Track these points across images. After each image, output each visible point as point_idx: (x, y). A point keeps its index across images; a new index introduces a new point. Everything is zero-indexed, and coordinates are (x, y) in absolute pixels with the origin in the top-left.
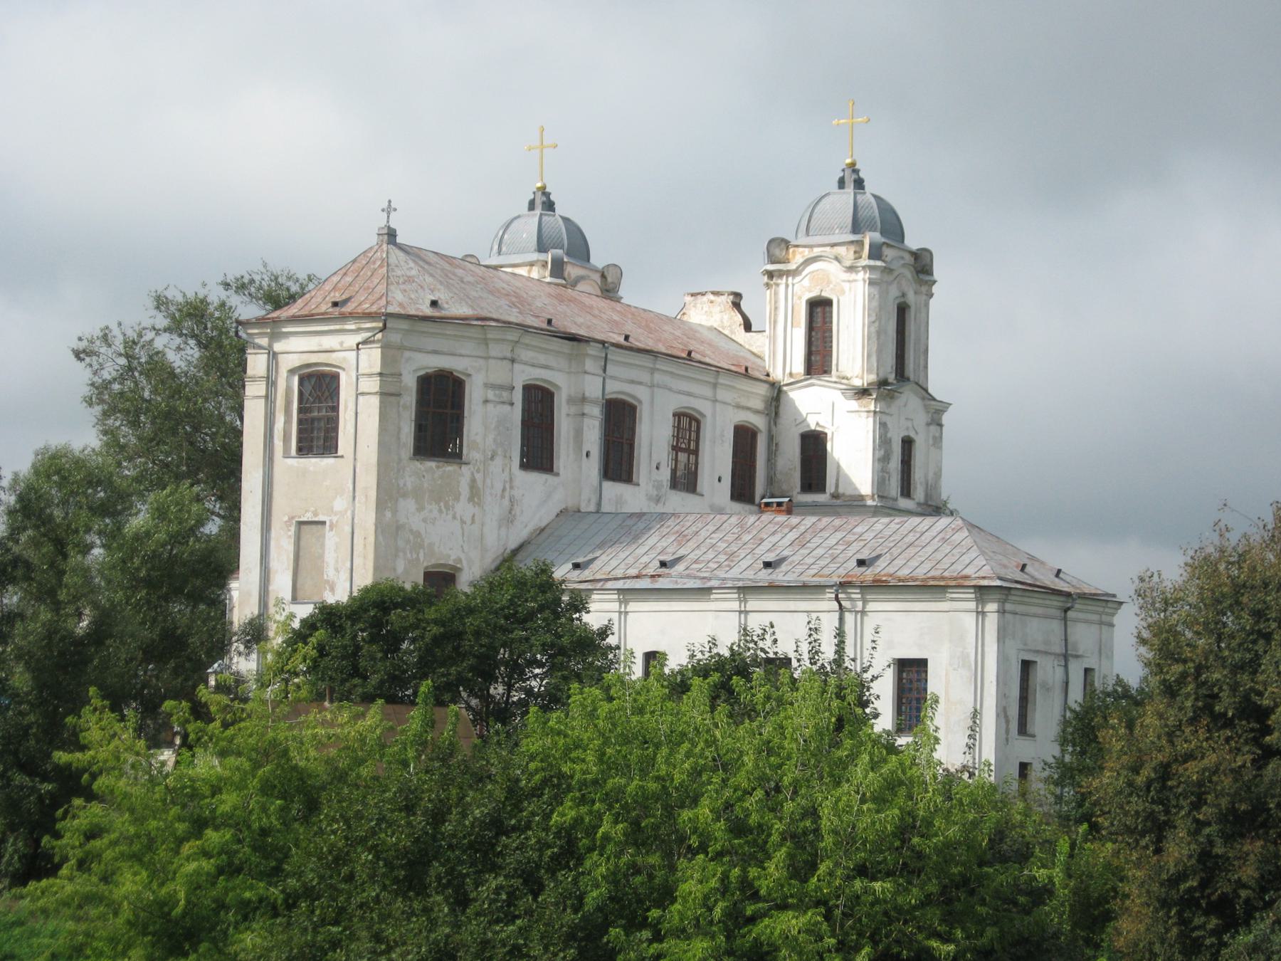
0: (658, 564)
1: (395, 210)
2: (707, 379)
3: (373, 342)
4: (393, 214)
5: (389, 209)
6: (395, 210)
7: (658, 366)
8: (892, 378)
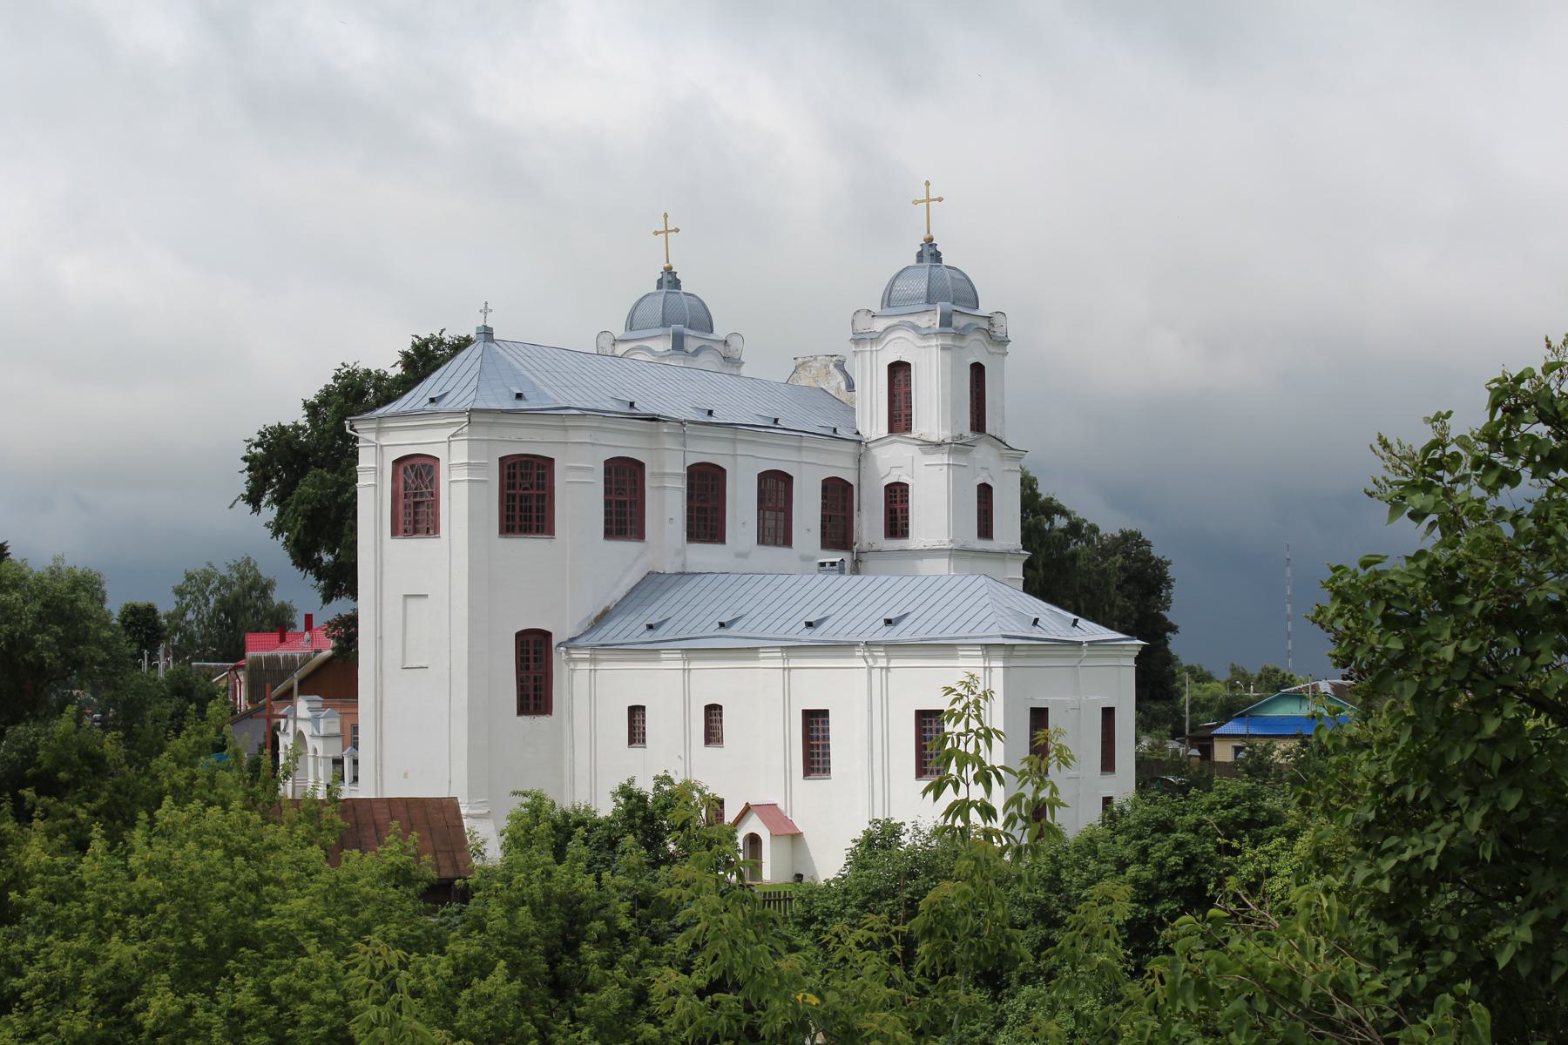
0: (718, 626)
3: (462, 434)
4: (489, 314)
5: (486, 310)
6: (491, 311)
8: (967, 431)
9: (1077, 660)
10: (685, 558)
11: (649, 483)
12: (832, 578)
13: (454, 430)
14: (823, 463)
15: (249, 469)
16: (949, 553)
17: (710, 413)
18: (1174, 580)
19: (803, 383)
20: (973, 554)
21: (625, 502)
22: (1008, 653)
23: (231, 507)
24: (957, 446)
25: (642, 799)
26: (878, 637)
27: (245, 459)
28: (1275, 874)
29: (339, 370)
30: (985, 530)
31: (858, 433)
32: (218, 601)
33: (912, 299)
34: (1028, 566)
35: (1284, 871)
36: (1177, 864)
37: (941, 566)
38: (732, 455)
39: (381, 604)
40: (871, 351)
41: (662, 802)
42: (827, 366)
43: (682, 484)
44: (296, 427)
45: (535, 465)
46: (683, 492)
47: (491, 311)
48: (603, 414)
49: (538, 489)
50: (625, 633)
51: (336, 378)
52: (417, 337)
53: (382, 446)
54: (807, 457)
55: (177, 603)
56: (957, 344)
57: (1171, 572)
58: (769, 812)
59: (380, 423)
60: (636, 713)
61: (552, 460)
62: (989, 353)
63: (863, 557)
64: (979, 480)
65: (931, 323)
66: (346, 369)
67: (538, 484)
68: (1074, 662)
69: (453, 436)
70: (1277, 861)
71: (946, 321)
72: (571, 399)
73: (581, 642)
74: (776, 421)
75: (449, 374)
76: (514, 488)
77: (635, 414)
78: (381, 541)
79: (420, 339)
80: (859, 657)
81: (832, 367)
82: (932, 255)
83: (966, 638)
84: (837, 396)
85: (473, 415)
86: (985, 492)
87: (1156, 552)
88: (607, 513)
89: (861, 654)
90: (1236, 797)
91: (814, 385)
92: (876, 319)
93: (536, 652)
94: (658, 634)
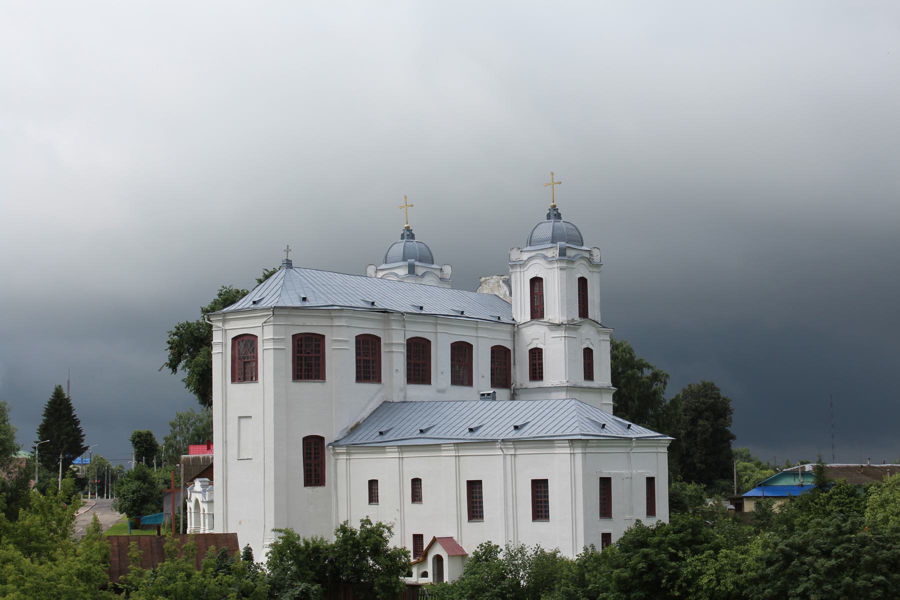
0: (419, 432)
1: (290, 250)
2: (472, 326)
3: (270, 322)
4: (289, 252)
5: (288, 250)
6: (290, 250)
7: (438, 322)
9: (630, 449)
10: (406, 394)
11: (383, 349)
12: (487, 402)
13: (265, 319)
14: (492, 337)
15: (171, 348)
16: (566, 388)
17: (421, 308)
18: (733, 409)
19: (485, 292)
20: (581, 389)
21: (369, 360)
22: (585, 445)
23: (160, 370)
24: (570, 326)
25: (354, 533)
26: (510, 436)
27: (169, 342)
28: (705, 573)
29: (221, 290)
30: (589, 374)
31: (513, 320)
32: (194, 430)
33: (542, 241)
34: (617, 397)
35: (710, 572)
36: (643, 568)
37: (563, 395)
38: (435, 333)
39: (226, 422)
40: (520, 272)
41: (364, 535)
42: (498, 282)
43: (403, 350)
44: (198, 323)
45: (314, 340)
46: (404, 355)
47: (285, 251)
48: (354, 309)
49: (316, 353)
50: (366, 438)
51: (220, 295)
52: (266, 270)
53: (226, 330)
54: (481, 333)
55: (171, 431)
56: (569, 266)
57: (732, 405)
58: (448, 542)
59: (224, 317)
60: (373, 484)
61: (323, 336)
62: (590, 271)
63: (517, 392)
64: (585, 346)
65: (554, 255)
66: (225, 290)
67: (315, 350)
68: (628, 450)
69: (265, 323)
70: (707, 565)
71: (563, 253)
72: (335, 300)
73: (341, 443)
74: (462, 313)
75: (265, 288)
76: (301, 353)
77: (374, 309)
78: (226, 385)
79: (268, 272)
80: (498, 449)
81: (501, 282)
82: (555, 215)
83: (560, 436)
84: (504, 299)
85: (275, 310)
86: (588, 354)
87: (723, 395)
88: (357, 367)
89: (499, 446)
90: (683, 526)
91: (491, 293)
92: (523, 253)
93: (315, 449)
94: (386, 437)
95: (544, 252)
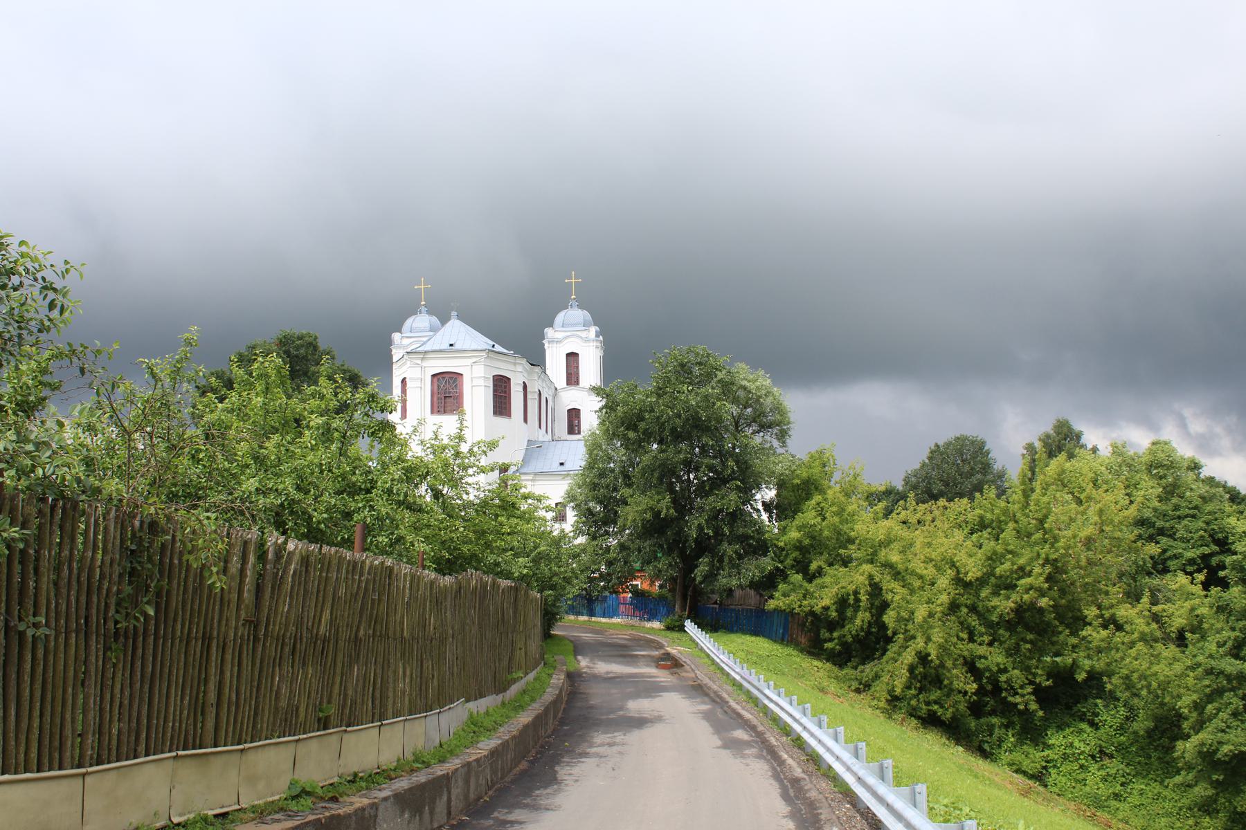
95: (579, 333)
